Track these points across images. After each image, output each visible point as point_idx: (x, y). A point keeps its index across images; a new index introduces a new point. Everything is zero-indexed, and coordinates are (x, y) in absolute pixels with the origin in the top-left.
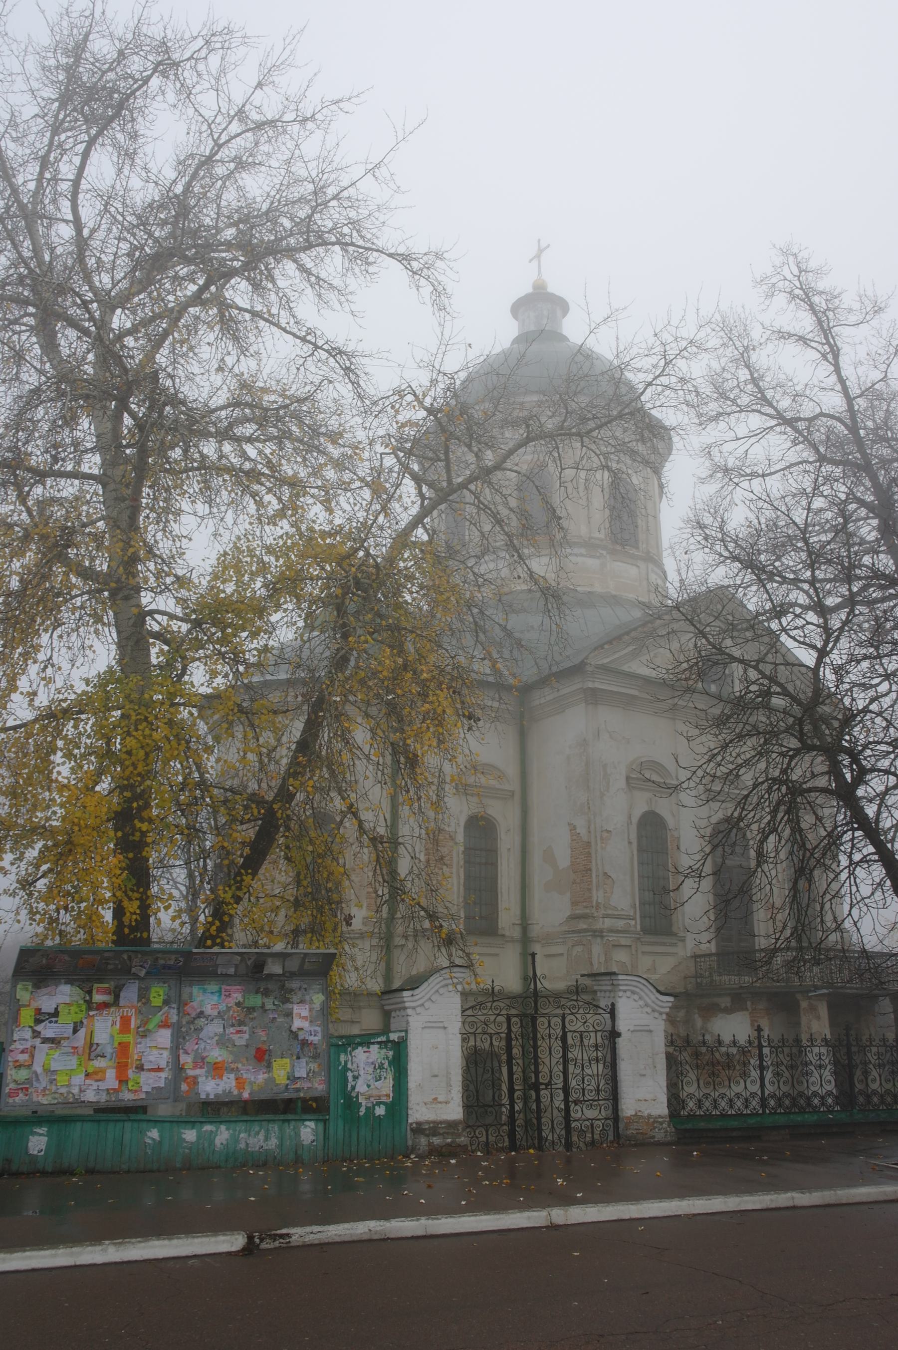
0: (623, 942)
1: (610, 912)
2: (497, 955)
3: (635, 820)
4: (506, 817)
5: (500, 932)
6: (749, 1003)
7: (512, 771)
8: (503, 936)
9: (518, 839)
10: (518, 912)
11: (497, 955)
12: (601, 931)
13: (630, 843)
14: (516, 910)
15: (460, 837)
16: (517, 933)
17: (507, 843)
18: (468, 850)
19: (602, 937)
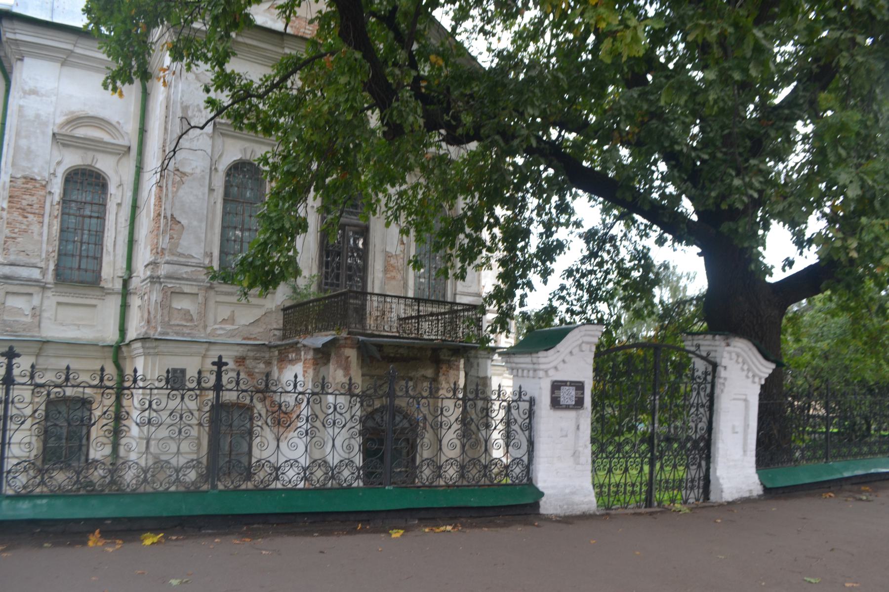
0: (187, 289)
1: (175, 259)
2: (95, 306)
3: (223, 166)
4: (117, 174)
5: (102, 284)
6: (303, 353)
7: (131, 127)
8: (103, 288)
9: (129, 194)
10: (125, 266)
11: (95, 306)
12: (159, 277)
13: (211, 190)
14: (122, 263)
15: (57, 187)
16: (118, 285)
17: (118, 195)
18: (65, 201)
19: (161, 283)
